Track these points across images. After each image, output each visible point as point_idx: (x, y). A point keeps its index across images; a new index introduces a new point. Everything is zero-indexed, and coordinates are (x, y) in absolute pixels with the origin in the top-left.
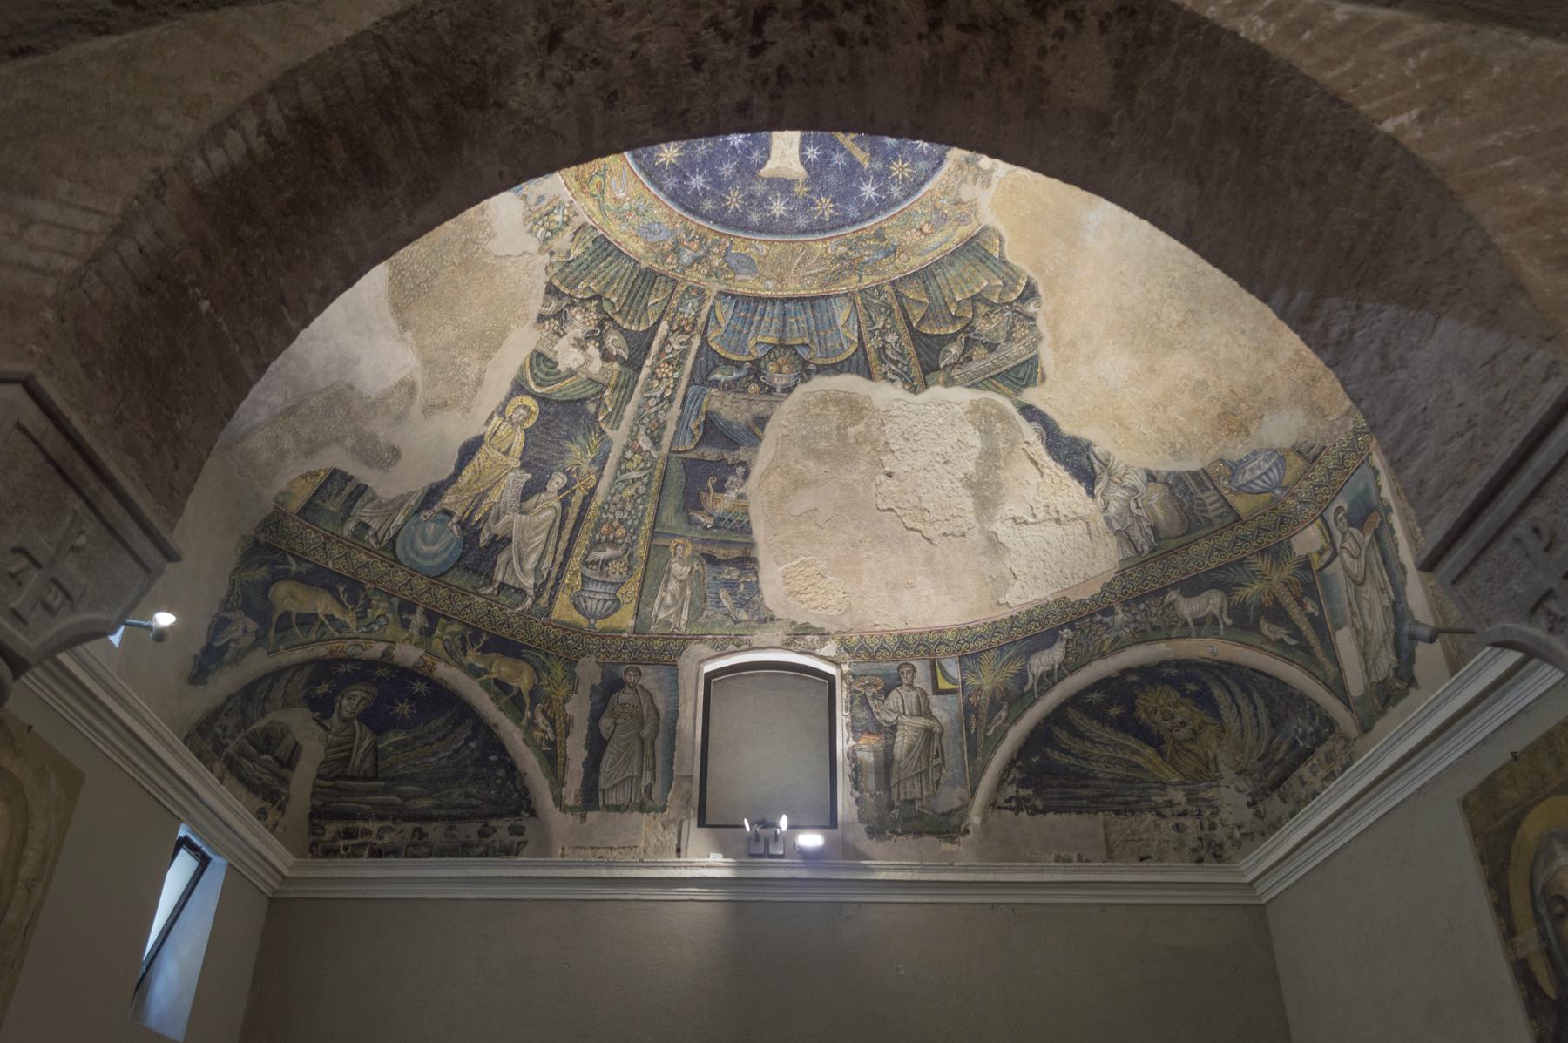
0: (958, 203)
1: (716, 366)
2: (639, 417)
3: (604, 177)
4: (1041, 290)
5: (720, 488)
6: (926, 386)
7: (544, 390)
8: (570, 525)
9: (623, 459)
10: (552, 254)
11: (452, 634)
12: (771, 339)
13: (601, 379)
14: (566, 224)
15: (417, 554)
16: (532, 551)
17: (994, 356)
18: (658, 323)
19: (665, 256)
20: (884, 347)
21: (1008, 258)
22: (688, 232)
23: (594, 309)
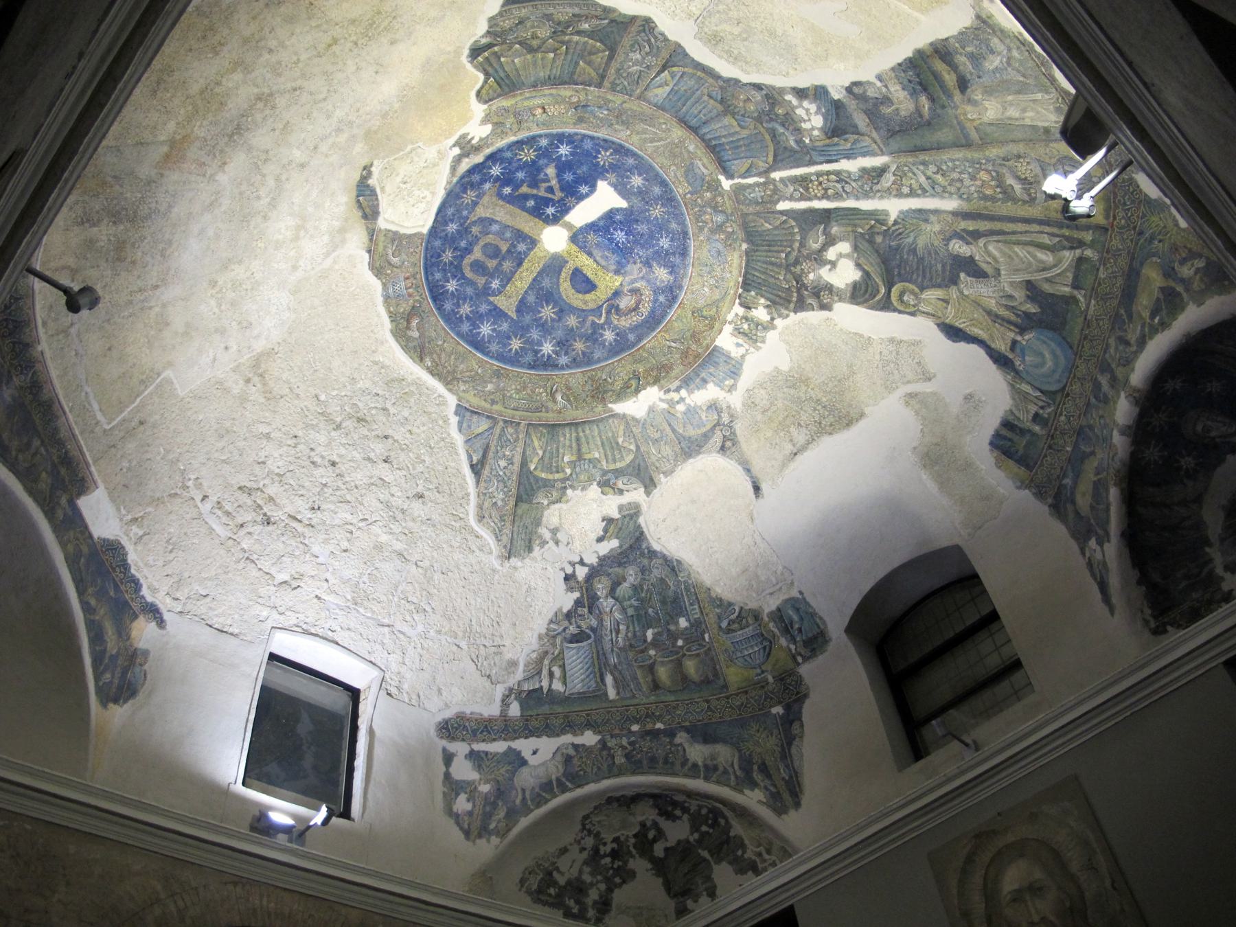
0: (495, 124)
1: (785, 148)
2: (866, 195)
3: (700, 310)
4: (466, 52)
5: (886, 100)
6: (634, 18)
7: (880, 283)
8: (997, 226)
9: (912, 194)
10: (773, 319)
11: (1116, 348)
12: (728, 120)
13: (852, 238)
14: (746, 319)
15: (1054, 371)
16: (1034, 257)
17: (551, 10)
18: (782, 213)
19: (729, 235)
20: (647, 54)
21: (481, 77)
22: (701, 229)
23: (798, 268)
